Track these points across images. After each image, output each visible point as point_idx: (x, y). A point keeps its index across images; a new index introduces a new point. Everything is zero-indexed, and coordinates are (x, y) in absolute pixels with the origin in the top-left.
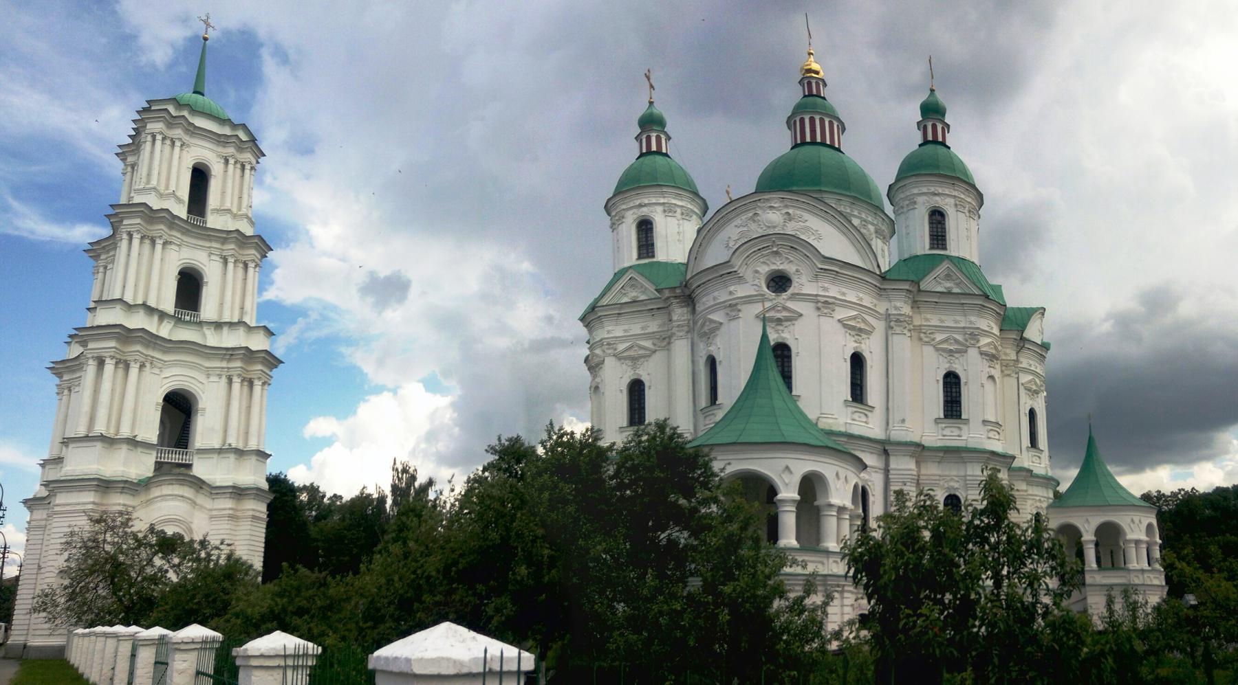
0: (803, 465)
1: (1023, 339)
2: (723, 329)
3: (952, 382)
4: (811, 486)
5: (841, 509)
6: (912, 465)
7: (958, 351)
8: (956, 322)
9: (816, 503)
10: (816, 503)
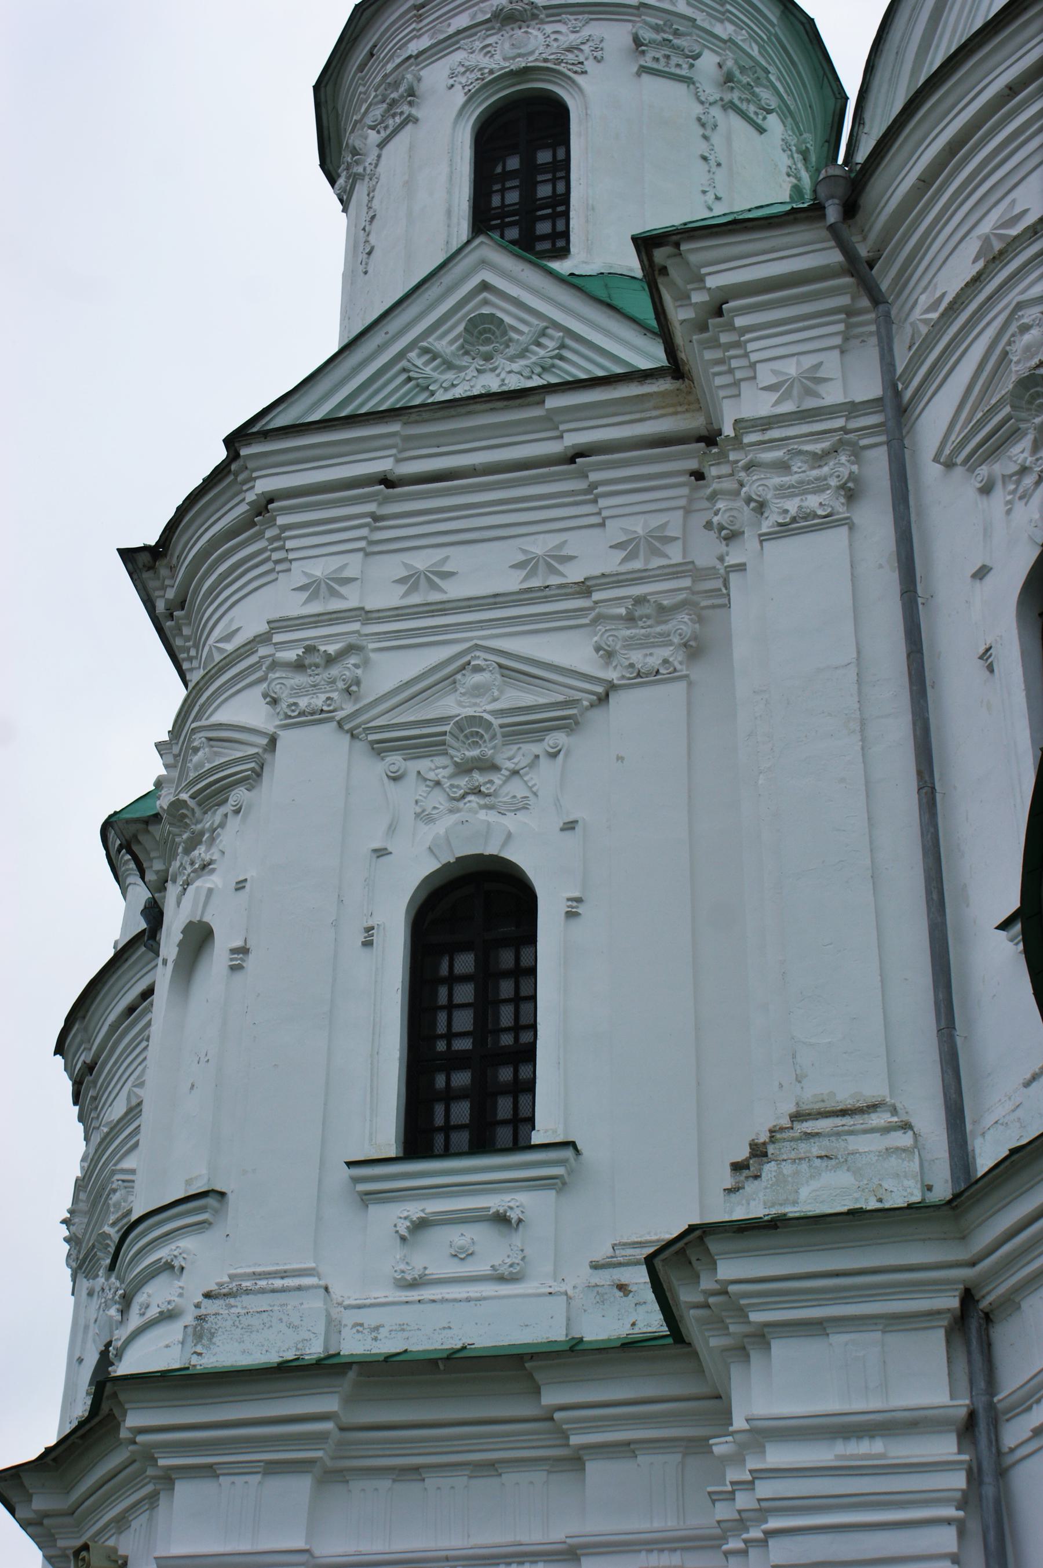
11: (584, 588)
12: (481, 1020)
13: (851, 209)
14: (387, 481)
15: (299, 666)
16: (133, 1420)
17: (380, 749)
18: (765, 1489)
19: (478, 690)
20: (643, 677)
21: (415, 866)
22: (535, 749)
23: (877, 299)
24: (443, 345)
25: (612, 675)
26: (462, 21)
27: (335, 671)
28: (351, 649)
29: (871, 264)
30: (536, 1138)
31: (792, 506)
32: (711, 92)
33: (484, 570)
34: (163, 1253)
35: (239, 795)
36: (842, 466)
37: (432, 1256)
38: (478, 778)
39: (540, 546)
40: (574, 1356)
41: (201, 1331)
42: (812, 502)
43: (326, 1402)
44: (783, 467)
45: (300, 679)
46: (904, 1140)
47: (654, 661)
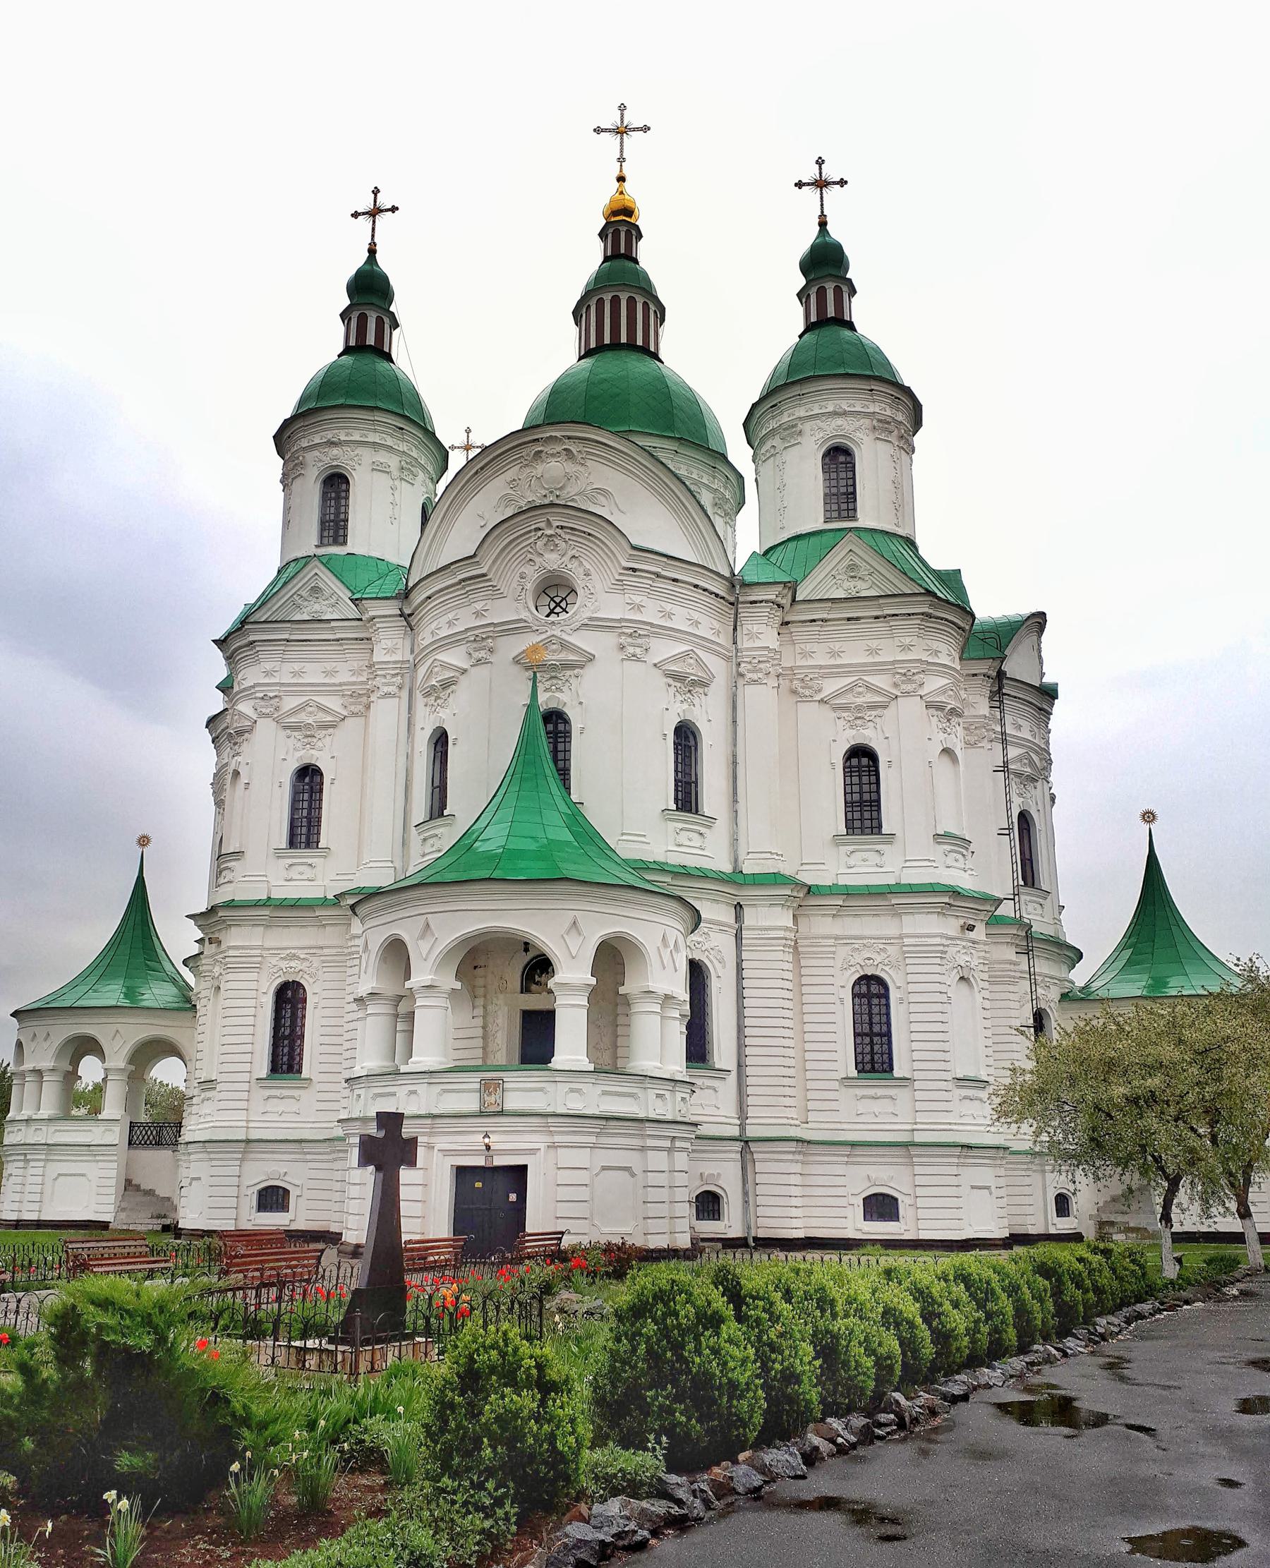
0: (602, 921)
1: (1001, 675)
2: (463, 680)
3: (861, 761)
4: (612, 958)
6: (784, 918)
7: (873, 707)
8: (873, 652)
9: (622, 990)
10: (622, 990)
11: (340, 684)
12: (310, 806)
17: (285, 728)
20: (354, 715)
21: (294, 765)
24: (303, 593)
27: (272, 702)
31: (386, 689)
32: (396, 473)
33: (313, 674)
34: (228, 864)
36: (398, 680)
37: (293, 873)
39: (329, 666)
40: (324, 903)
45: (263, 703)
47: (356, 711)
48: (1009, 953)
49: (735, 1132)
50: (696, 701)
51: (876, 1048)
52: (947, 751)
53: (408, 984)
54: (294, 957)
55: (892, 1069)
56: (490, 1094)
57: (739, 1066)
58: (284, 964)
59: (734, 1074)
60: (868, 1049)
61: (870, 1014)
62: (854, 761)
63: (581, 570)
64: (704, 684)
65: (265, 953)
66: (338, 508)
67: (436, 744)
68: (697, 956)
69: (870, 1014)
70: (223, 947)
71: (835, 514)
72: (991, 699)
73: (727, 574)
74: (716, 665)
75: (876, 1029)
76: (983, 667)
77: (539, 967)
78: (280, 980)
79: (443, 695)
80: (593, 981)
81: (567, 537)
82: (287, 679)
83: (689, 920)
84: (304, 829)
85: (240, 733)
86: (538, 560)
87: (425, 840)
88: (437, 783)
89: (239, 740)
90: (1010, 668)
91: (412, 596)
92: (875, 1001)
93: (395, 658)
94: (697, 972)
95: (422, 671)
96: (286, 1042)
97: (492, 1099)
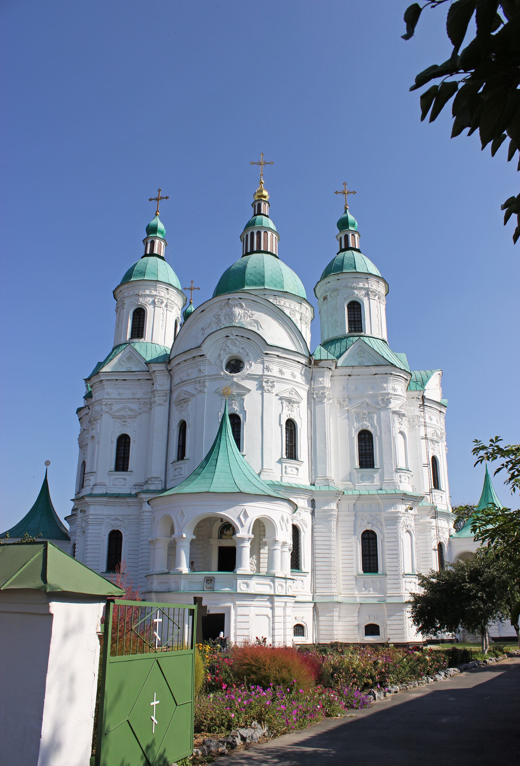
1: (423, 397)
5: (284, 544)
11: (138, 399)
13: (169, 362)
14: (117, 380)
15: (105, 405)
16: (86, 500)
17: (114, 418)
18: (144, 517)
19: (125, 411)
21: (118, 434)
22: (131, 420)
23: (171, 376)
24: (124, 359)
25: (140, 411)
26: (131, 293)
28: (111, 404)
29: (170, 370)
30: (129, 470)
35: (99, 421)
36: (164, 398)
38: (125, 423)
40: (130, 496)
41: (92, 489)
42: (161, 402)
43: (105, 499)
44: (159, 396)
46: (160, 482)
48: (428, 519)
49: (311, 600)
50: (295, 410)
51: (371, 561)
52: (401, 433)
53: (173, 536)
54: (117, 519)
55: (378, 570)
56: (208, 583)
57: (313, 570)
58: (113, 522)
59: (310, 574)
60: (368, 562)
61: (369, 547)
62: (363, 436)
63: (245, 353)
64: (298, 403)
65: (104, 517)
66: (139, 321)
67: (180, 427)
68: (295, 523)
69: (369, 547)
70: (87, 514)
71: (353, 329)
72: (420, 407)
73: (308, 355)
74: (304, 394)
75: (372, 553)
76: (416, 394)
77: (228, 528)
78: (111, 530)
79: (184, 405)
80: (253, 536)
81: (240, 340)
82: (117, 397)
83: (293, 509)
84: (122, 463)
85: (95, 420)
86: (227, 349)
87: (175, 469)
88: (181, 444)
89: (95, 423)
90: (427, 395)
91: (172, 362)
92: (371, 541)
93: (163, 388)
94: (296, 531)
95: (175, 395)
96: (113, 557)
97: (209, 586)
